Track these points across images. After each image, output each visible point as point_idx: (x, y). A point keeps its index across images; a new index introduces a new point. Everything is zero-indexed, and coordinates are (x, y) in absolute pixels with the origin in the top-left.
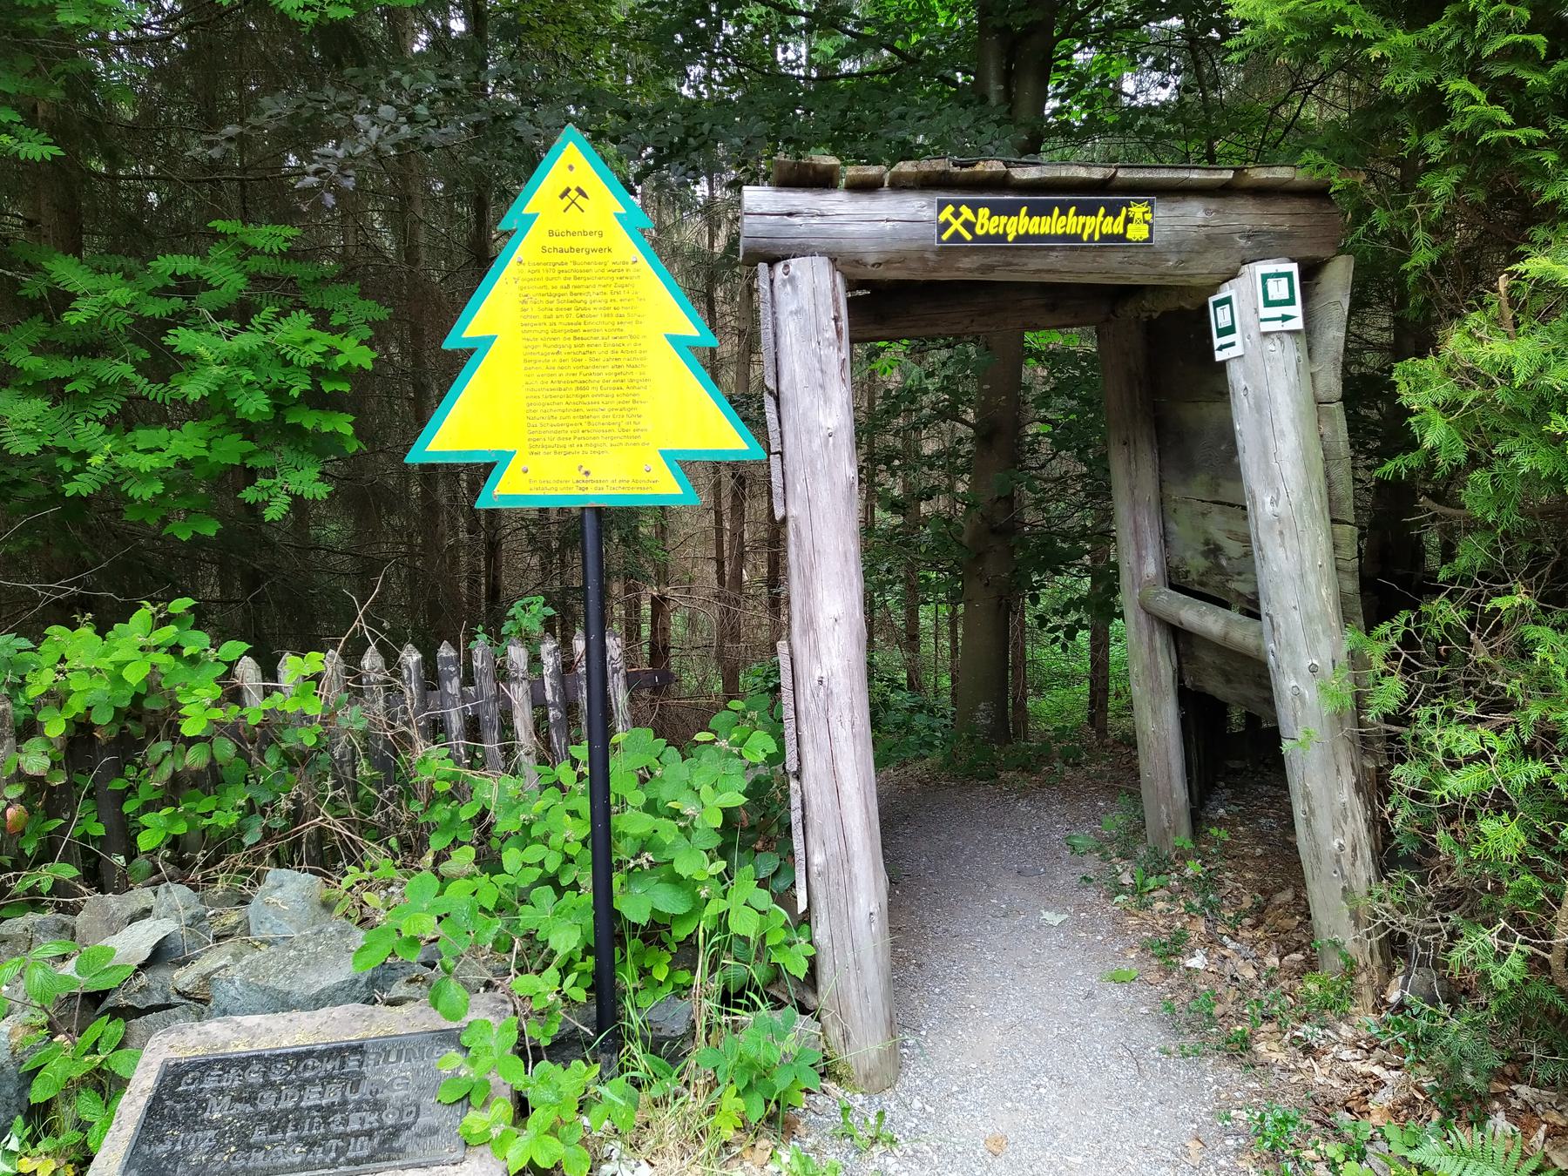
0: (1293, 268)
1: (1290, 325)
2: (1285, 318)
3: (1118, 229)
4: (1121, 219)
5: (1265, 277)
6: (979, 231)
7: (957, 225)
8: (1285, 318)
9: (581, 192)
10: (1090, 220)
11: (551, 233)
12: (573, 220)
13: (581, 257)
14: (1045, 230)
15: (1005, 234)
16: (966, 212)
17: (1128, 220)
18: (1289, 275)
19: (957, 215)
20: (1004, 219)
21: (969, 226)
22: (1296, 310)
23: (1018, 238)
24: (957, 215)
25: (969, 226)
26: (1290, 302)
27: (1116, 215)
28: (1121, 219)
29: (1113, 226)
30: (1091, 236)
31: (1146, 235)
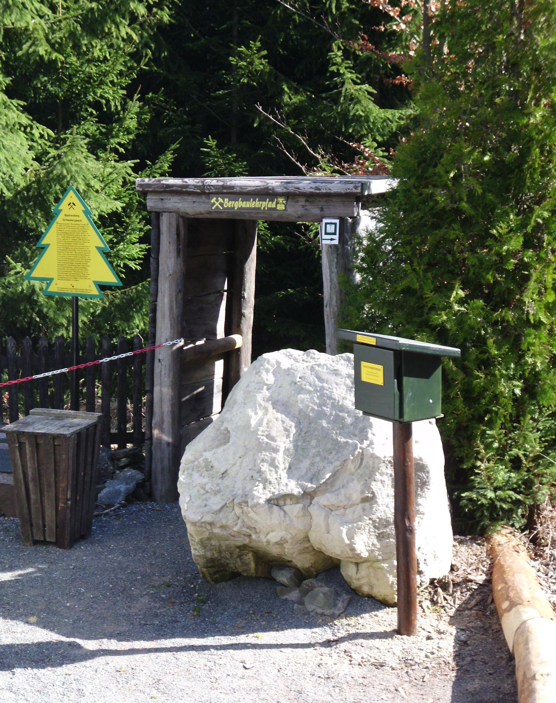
0: (337, 221)
1: (334, 242)
2: (332, 239)
3: (274, 206)
4: (275, 203)
5: (326, 224)
6: (225, 206)
7: (217, 204)
8: (332, 239)
9: (74, 204)
10: (264, 203)
11: (66, 215)
12: (72, 212)
13: (73, 222)
14: (248, 206)
15: (234, 207)
16: (220, 200)
17: (277, 203)
18: (335, 224)
19: (217, 200)
20: (233, 202)
21: (221, 204)
22: (336, 237)
23: (238, 208)
24: (217, 200)
25: (221, 204)
26: (335, 234)
27: (273, 201)
28: (275, 203)
29: (272, 205)
30: (264, 208)
31: (284, 208)
